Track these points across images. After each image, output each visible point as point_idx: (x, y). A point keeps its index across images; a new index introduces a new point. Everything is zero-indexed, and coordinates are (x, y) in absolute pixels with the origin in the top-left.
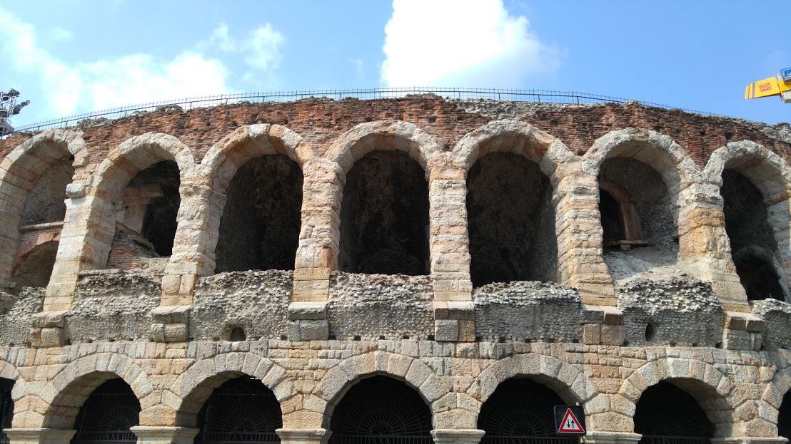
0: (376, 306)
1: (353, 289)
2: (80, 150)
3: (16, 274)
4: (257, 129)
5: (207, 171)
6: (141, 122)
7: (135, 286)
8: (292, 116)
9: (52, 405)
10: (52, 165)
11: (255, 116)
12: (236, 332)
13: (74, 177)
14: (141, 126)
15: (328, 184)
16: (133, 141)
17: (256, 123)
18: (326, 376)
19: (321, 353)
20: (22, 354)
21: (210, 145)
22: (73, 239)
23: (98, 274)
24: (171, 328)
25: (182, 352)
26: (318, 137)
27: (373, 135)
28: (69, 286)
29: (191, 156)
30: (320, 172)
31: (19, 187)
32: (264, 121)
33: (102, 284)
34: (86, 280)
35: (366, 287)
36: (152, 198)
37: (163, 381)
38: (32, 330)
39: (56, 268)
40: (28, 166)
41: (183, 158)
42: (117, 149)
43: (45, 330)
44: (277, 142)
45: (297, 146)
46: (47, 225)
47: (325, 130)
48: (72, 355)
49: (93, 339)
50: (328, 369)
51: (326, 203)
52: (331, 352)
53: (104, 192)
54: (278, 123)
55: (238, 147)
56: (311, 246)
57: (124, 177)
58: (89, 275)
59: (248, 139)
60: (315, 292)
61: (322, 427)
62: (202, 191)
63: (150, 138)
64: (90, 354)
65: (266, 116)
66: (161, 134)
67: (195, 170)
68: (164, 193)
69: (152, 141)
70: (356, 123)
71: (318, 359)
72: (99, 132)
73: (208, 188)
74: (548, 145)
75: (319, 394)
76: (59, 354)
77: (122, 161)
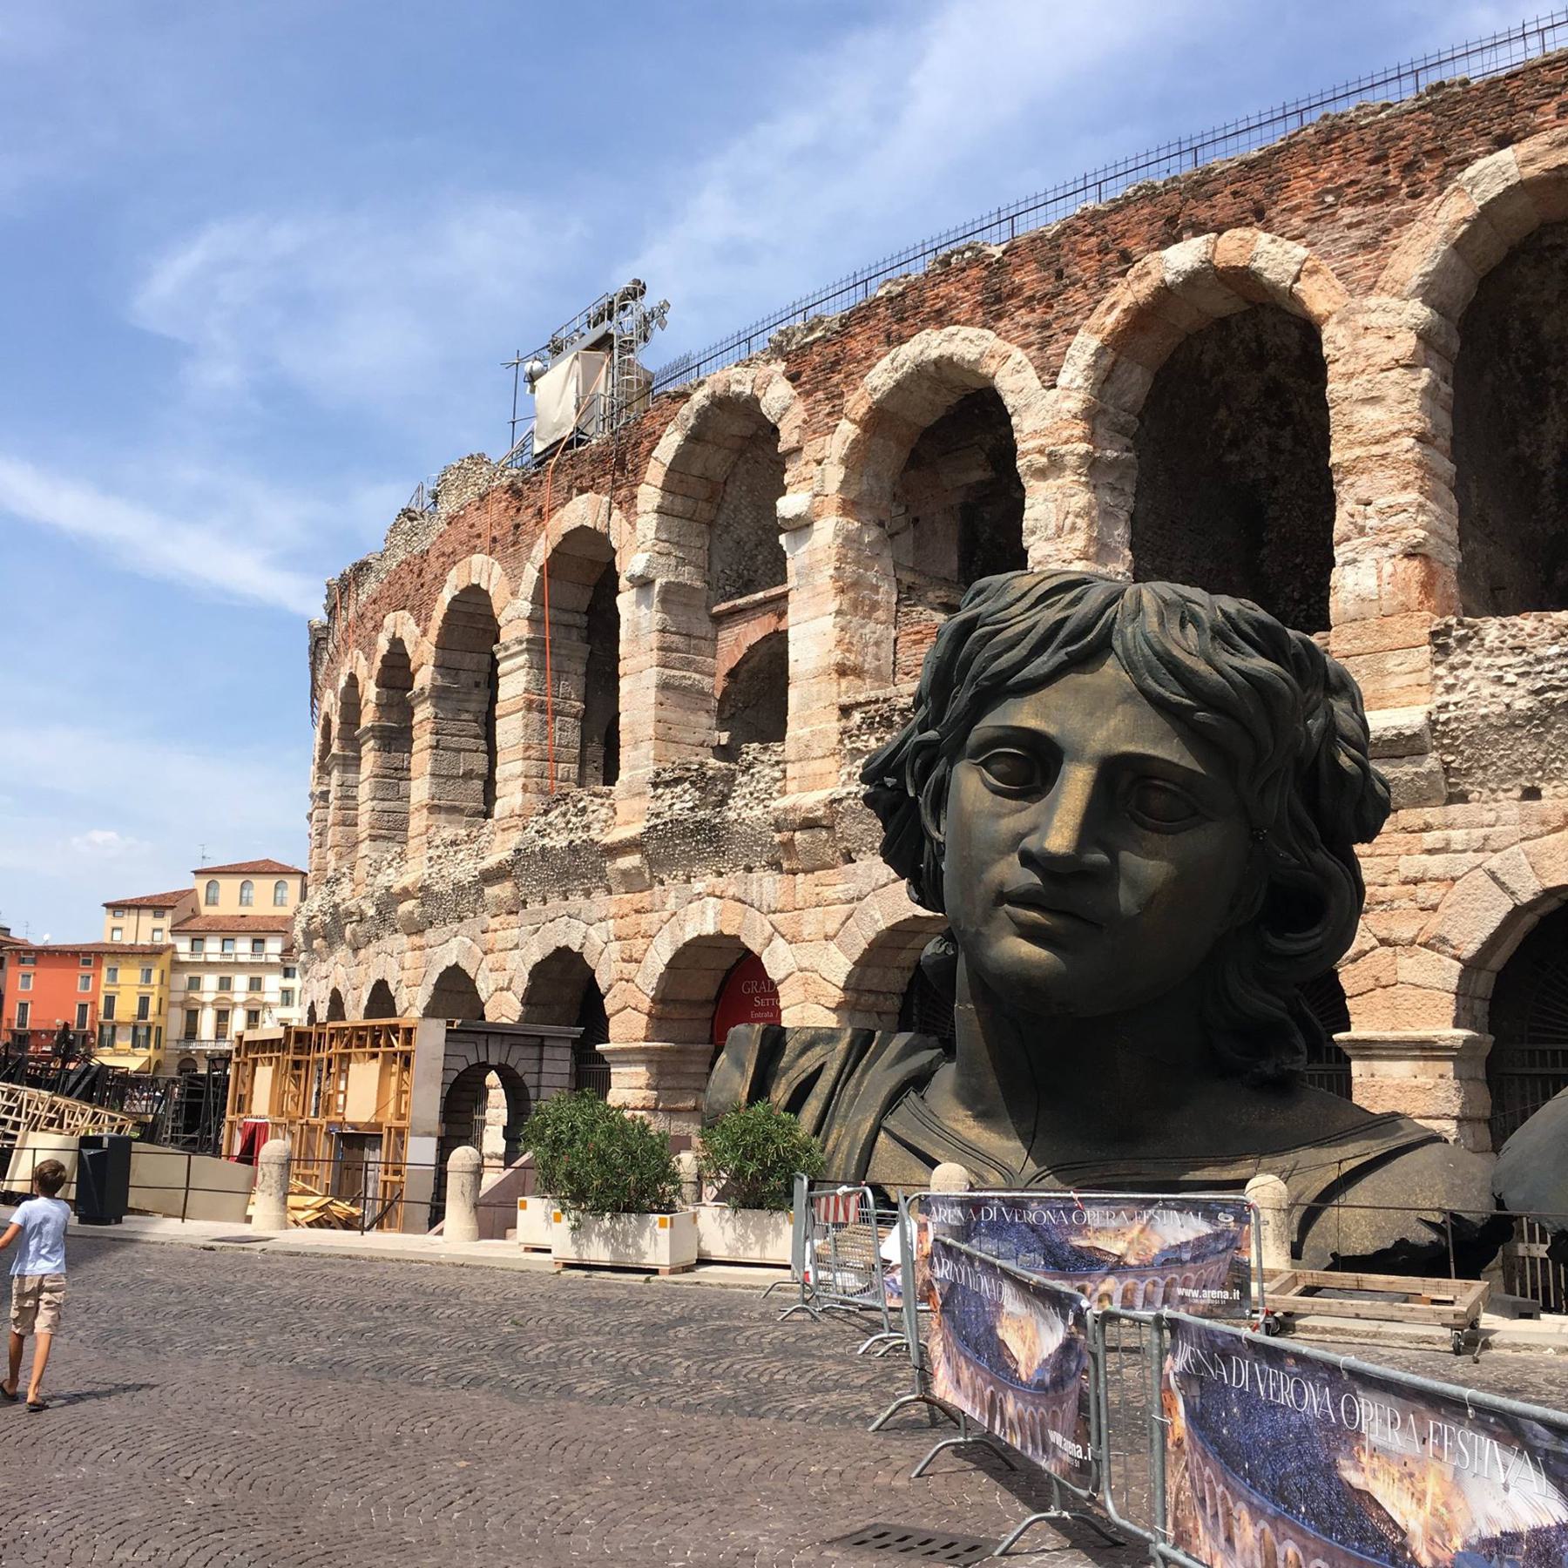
1: (1502, 661)
2: (786, 409)
3: (726, 714)
4: (1184, 256)
5: (1075, 404)
6: (905, 310)
8: (1272, 192)
9: (844, 989)
10: (741, 452)
11: (1171, 221)
13: (787, 478)
14: (902, 320)
15: (1396, 374)
16: (893, 360)
17: (1177, 239)
18: (1451, 898)
19: (1430, 839)
20: (767, 885)
21: (1073, 331)
23: (877, 701)
26: (1356, 234)
27: (1523, 186)
29: (1031, 372)
30: (1370, 342)
31: (690, 519)
32: (1198, 229)
34: (857, 717)
35: (1541, 652)
36: (970, 487)
38: (778, 838)
40: (697, 468)
41: (1015, 380)
42: (861, 390)
43: (798, 835)
44: (1243, 280)
45: (1297, 279)
46: (760, 595)
47: (1371, 209)
50: (1454, 880)
51: (1395, 428)
52: (1458, 837)
53: (854, 503)
54: (1239, 223)
55: (1141, 318)
56: (1367, 561)
57: (892, 456)
58: (858, 705)
59: (1164, 293)
60: (1393, 684)
61: (1456, 1025)
62: (1071, 460)
63: (929, 344)
65: (1203, 213)
66: (952, 329)
67: (1048, 405)
68: (994, 469)
69: (934, 354)
70: (1465, 162)
71: (1425, 857)
72: (817, 359)
73: (1083, 447)
75: (1436, 944)
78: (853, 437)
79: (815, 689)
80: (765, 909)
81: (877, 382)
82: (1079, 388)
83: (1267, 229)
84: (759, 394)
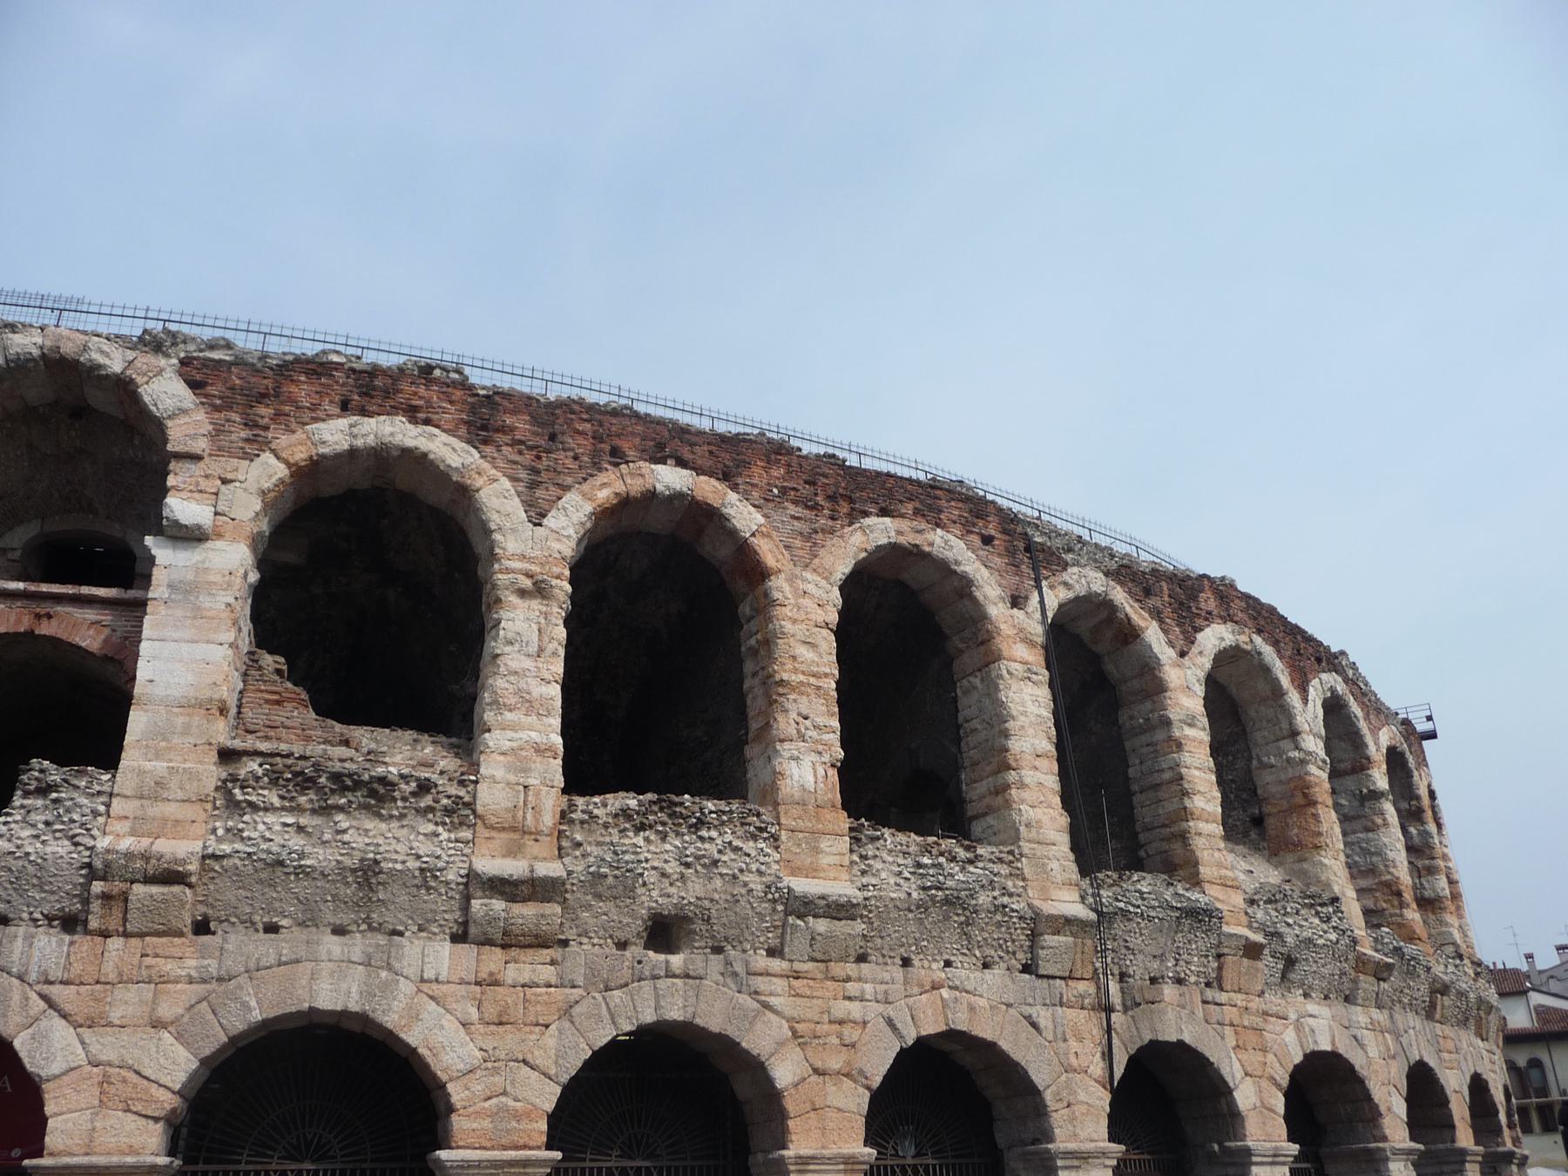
0: (947, 901)
4: (670, 478)
7: (404, 799)
12: (664, 932)
13: (171, 481)
16: (351, 426)
22: (185, 647)
24: (526, 913)
25: (548, 973)
28: (193, 776)
30: (805, 602)
33: (305, 782)
37: (508, 1041)
39: (137, 722)
41: (500, 500)
43: (139, 889)
48: (232, 964)
49: (284, 922)
60: (825, 860)
64: (286, 963)
67: (533, 540)
70: (866, 514)
74: (1142, 629)
76: (185, 959)
77: (309, 473)
78: (280, 475)
79: (180, 721)
80: (33, 977)
81: (327, 437)
82: (569, 537)
83: (734, 487)
84: (139, 380)
